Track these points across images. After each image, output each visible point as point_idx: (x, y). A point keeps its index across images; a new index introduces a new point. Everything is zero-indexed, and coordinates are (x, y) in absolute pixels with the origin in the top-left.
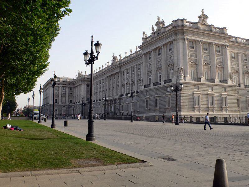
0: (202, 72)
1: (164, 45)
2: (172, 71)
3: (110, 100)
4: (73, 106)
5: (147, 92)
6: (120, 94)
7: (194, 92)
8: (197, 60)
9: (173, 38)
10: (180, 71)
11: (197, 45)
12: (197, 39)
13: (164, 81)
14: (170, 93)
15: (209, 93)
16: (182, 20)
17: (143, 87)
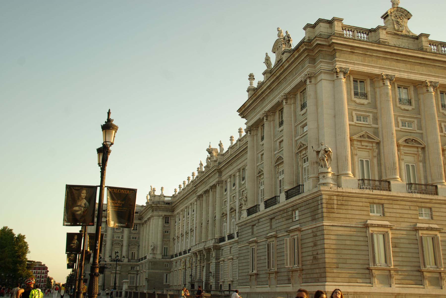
0: (394, 163)
1: (287, 97)
2: (305, 165)
3: (200, 251)
4: (138, 265)
5: (253, 226)
6: (217, 236)
7: (369, 222)
8: (378, 128)
9: (307, 69)
10: (323, 160)
11: (377, 90)
12: (376, 71)
13: (287, 192)
14: (298, 226)
15: (419, 225)
16: (330, 23)
17: (245, 214)
